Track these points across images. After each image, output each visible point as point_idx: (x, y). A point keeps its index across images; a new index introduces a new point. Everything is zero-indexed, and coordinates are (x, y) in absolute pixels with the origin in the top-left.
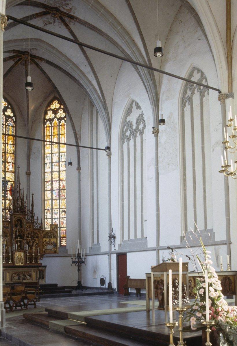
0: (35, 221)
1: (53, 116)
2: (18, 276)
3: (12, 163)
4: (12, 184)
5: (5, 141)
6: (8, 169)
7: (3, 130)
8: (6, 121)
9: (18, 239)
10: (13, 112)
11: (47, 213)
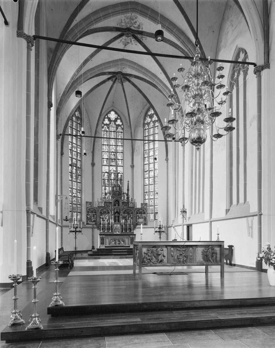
1: (150, 120)
4: (122, 175)
5: (116, 143)
8: (117, 128)
9: (116, 214)
10: (121, 121)
11: (146, 195)
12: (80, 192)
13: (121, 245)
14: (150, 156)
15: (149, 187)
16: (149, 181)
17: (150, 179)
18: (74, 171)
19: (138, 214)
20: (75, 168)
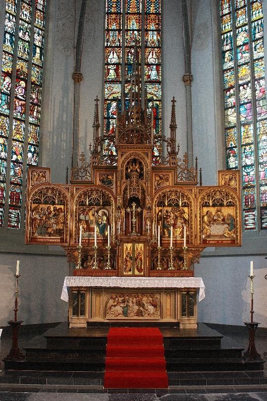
0: (179, 164)
2: (122, 305)
3: (158, 65)
6: (149, 76)
7: (138, 7)
9: (131, 207)
12: (34, 152)
13: (146, 318)
14: (240, 46)
15: (239, 132)
16: (239, 113)
17: (242, 109)
18: (20, 92)
19: (205, 209)
20: (23, 84)
